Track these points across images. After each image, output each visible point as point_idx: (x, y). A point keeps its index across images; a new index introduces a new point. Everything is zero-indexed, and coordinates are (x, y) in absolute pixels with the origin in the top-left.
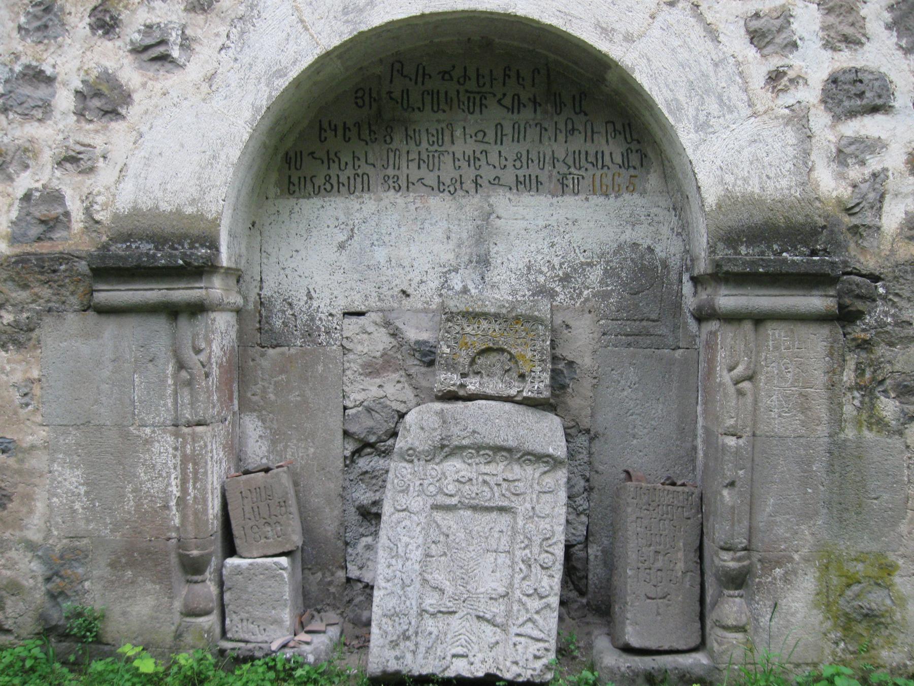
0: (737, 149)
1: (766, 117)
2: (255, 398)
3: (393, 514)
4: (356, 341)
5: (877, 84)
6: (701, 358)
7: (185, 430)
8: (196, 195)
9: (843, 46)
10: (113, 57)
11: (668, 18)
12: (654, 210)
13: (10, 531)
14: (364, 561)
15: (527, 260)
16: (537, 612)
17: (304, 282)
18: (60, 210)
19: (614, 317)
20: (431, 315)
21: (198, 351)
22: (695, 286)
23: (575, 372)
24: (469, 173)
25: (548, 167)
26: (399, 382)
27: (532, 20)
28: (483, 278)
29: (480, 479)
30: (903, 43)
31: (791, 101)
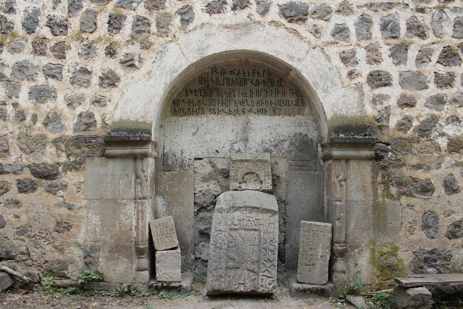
0: (338, 99)
1: (348, 88)
2: (161, 190)
5: (386, 76)
6: (325, 174)
7: (139, 201)
8: (143, 115)
9: (374, 63)
10: (113, 65)
11: (313, 53)
12: (307, 121)
13: (71, 239)
16: (269, 267)
17: (180, 147)
18: (93, 120)
21: (144, 172)
22: (322, 148)
24: (240, 108)
25: (269, 106)
27: (265, 53)
30: (395, 62)
31: (356, 82)
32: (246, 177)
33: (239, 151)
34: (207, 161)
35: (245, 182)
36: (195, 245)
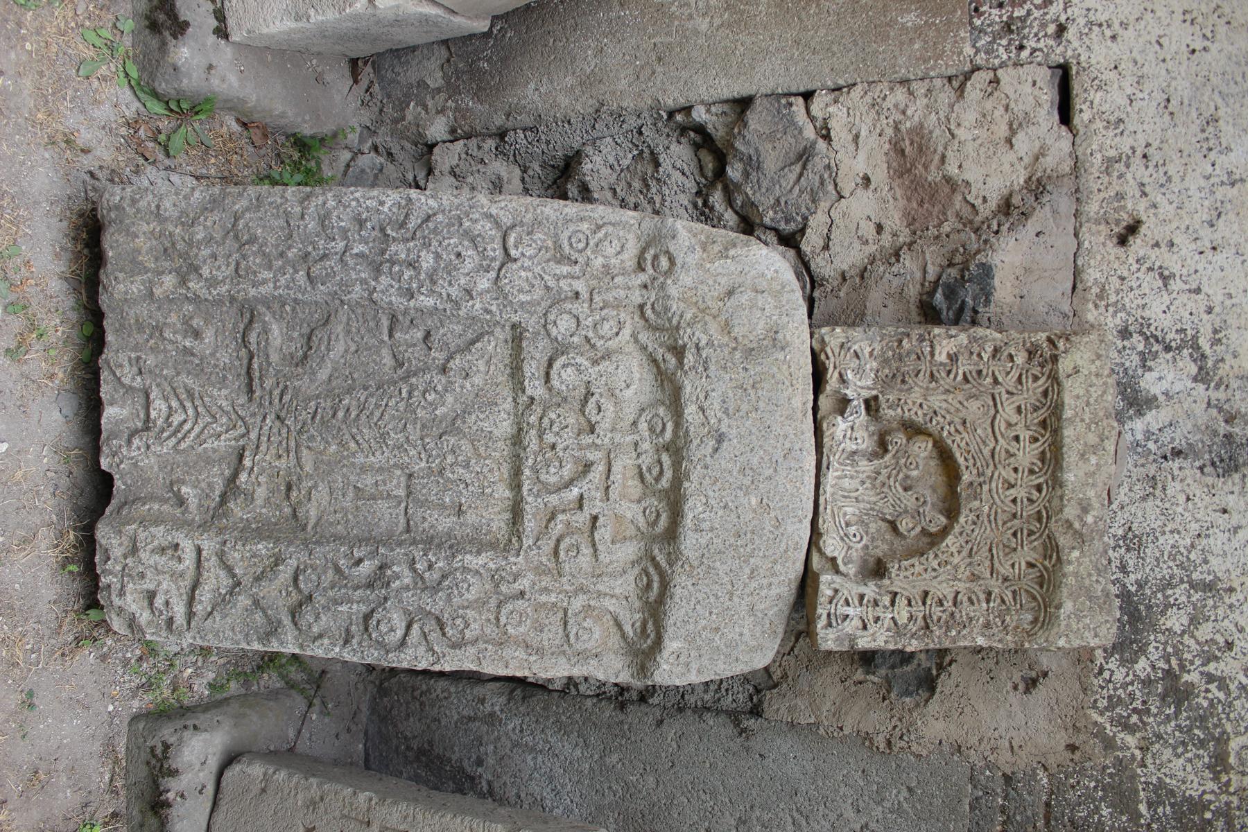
3: (497, 224)
4: (988, 105)
14: (470, 179)
15: (1236, 585)
19: (1056, 811)
20: (1066, 308)
23: (907, 693)
26: (879, 228)
28: (1177, 453)
29: (592, 456)
32: (922, 449)
33: (1135, 401)
34: (1049, 162)
35: (883, 446)
36: (502, 135)
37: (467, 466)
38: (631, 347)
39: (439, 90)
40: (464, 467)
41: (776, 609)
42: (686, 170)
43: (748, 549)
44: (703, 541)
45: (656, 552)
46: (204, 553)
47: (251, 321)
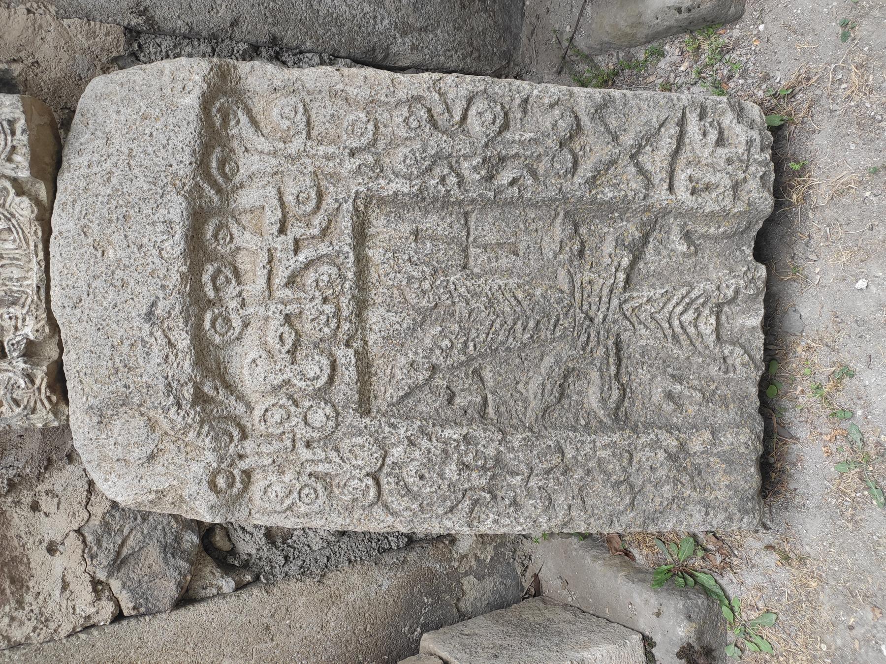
3: (386, 507)
26: (35, 507)
29: (287, 293)
37: (410, 279)
38: (253, 398)
39: (466, 574)
40: (413, 277)
41: (82, 140)
42: (240, 533)
43: (114, 203)
44: (162, 211)
45: (216, 199)
46: (666, 186)
47: (617, 409)
